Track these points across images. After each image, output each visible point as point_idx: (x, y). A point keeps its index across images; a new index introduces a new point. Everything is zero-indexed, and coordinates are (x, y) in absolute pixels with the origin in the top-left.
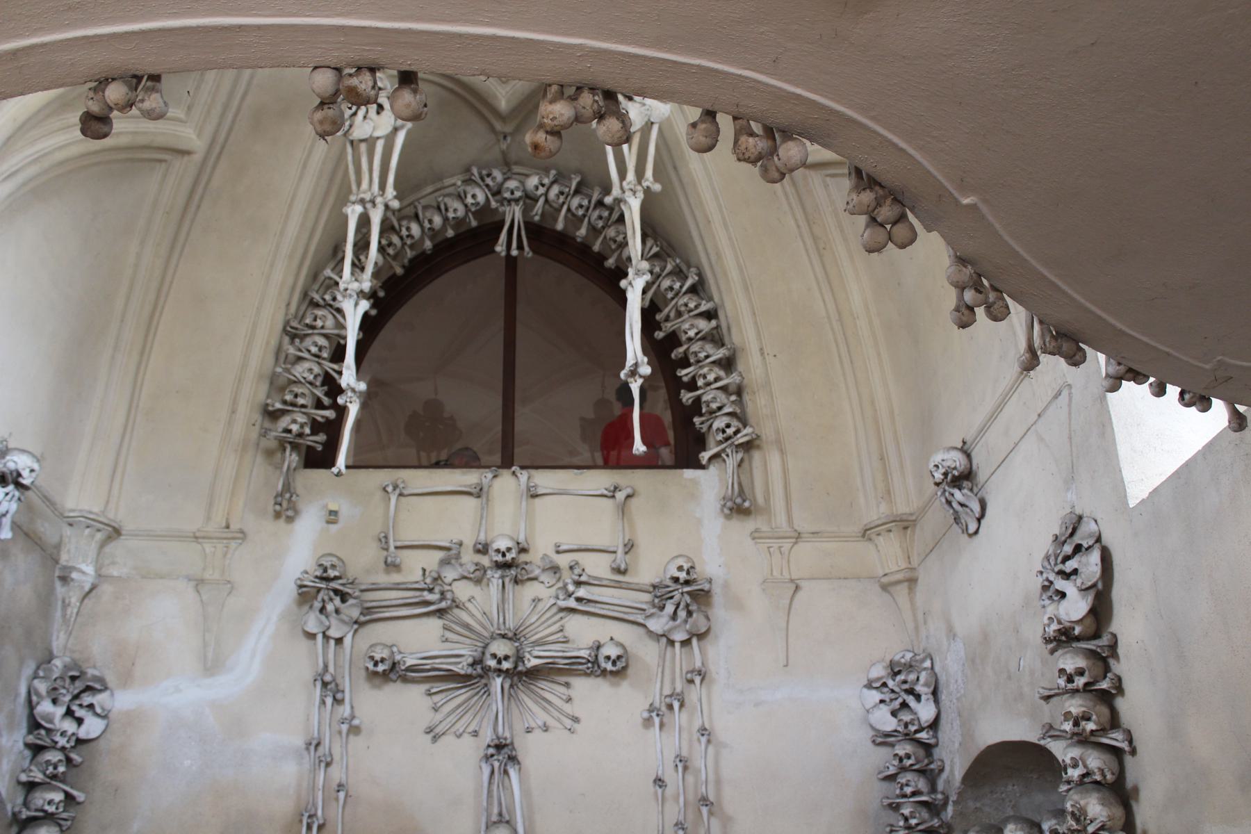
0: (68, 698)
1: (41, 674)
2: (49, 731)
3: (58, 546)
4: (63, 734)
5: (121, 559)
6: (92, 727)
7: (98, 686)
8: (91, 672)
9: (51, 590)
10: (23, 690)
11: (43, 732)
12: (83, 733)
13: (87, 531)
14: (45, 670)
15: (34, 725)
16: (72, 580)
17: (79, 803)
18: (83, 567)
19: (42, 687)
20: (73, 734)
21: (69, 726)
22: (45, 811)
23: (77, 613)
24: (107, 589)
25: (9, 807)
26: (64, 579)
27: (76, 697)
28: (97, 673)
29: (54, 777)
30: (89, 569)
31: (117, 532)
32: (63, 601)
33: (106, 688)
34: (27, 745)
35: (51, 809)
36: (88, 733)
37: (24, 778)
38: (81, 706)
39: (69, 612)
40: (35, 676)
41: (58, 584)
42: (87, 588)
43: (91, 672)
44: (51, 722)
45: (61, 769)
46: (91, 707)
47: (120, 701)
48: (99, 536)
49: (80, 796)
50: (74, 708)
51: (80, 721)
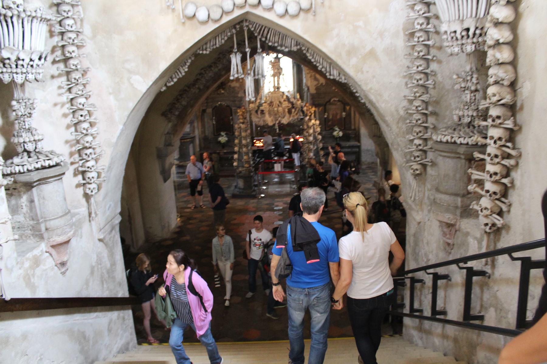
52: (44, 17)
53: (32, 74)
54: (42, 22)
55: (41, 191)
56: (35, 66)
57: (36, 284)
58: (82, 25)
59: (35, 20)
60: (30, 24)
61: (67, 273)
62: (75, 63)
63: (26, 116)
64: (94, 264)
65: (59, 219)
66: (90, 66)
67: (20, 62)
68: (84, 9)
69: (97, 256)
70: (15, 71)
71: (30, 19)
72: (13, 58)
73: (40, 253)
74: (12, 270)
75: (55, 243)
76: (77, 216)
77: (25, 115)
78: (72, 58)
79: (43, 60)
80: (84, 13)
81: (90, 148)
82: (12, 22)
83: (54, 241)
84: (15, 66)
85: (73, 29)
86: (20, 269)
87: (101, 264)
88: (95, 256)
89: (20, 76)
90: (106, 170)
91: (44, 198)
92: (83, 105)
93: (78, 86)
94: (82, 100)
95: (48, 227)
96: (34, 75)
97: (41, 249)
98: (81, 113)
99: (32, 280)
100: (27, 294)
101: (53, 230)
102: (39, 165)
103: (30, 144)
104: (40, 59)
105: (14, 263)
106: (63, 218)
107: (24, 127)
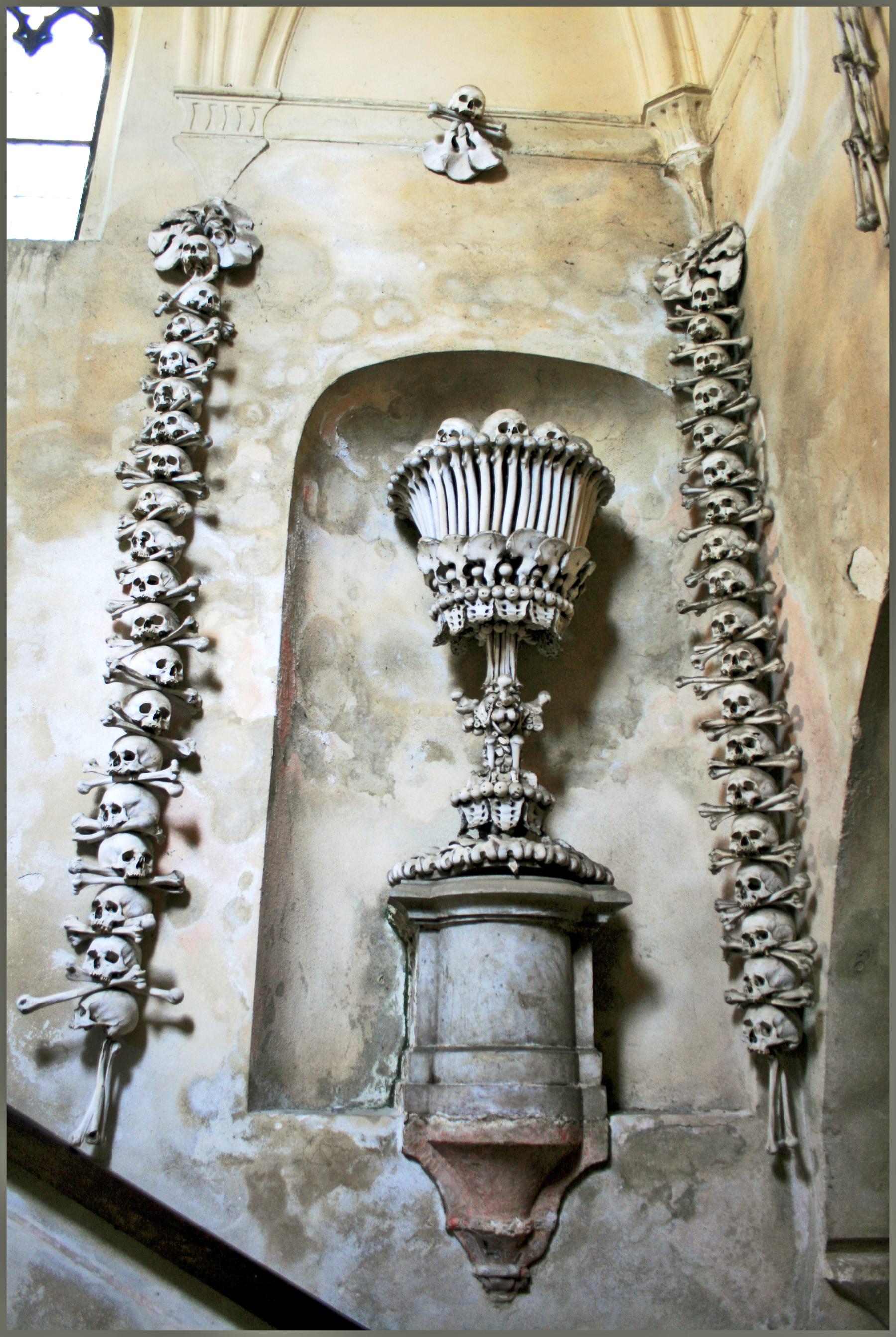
1: (664, 260)
2: (686, 302)
3: (655, 148)
4: (698, 294)
9: (662, 189)
11: (679, 307)
14: (673, 257)
15: (670, 306)
16: (673, 165)
18: (682, 147)
19: (668, 271)
21: (704, 285)
26: (670, 173)
27: (706, 252)
34: (673, 327)
36: (729, 279)
38: (709, 261)
39: (695, 195)
42: (697, 162)
46: (723, 255)
48: (681, 109)
57: (309, 1233)
59: (482, 459)
61: (522, 1301)
65: (466, 1055)
67: (450, 575)
73: (375, 1145)
74: (205, 1121)
79: (526, 566)
85: (722, 475)
86: (247, 1139)
95: (437, 1074)
96: (491, 607)
97: (384, 1132)
99: (293, 1207)
105: (225, 1107)
106: (485, 1056)
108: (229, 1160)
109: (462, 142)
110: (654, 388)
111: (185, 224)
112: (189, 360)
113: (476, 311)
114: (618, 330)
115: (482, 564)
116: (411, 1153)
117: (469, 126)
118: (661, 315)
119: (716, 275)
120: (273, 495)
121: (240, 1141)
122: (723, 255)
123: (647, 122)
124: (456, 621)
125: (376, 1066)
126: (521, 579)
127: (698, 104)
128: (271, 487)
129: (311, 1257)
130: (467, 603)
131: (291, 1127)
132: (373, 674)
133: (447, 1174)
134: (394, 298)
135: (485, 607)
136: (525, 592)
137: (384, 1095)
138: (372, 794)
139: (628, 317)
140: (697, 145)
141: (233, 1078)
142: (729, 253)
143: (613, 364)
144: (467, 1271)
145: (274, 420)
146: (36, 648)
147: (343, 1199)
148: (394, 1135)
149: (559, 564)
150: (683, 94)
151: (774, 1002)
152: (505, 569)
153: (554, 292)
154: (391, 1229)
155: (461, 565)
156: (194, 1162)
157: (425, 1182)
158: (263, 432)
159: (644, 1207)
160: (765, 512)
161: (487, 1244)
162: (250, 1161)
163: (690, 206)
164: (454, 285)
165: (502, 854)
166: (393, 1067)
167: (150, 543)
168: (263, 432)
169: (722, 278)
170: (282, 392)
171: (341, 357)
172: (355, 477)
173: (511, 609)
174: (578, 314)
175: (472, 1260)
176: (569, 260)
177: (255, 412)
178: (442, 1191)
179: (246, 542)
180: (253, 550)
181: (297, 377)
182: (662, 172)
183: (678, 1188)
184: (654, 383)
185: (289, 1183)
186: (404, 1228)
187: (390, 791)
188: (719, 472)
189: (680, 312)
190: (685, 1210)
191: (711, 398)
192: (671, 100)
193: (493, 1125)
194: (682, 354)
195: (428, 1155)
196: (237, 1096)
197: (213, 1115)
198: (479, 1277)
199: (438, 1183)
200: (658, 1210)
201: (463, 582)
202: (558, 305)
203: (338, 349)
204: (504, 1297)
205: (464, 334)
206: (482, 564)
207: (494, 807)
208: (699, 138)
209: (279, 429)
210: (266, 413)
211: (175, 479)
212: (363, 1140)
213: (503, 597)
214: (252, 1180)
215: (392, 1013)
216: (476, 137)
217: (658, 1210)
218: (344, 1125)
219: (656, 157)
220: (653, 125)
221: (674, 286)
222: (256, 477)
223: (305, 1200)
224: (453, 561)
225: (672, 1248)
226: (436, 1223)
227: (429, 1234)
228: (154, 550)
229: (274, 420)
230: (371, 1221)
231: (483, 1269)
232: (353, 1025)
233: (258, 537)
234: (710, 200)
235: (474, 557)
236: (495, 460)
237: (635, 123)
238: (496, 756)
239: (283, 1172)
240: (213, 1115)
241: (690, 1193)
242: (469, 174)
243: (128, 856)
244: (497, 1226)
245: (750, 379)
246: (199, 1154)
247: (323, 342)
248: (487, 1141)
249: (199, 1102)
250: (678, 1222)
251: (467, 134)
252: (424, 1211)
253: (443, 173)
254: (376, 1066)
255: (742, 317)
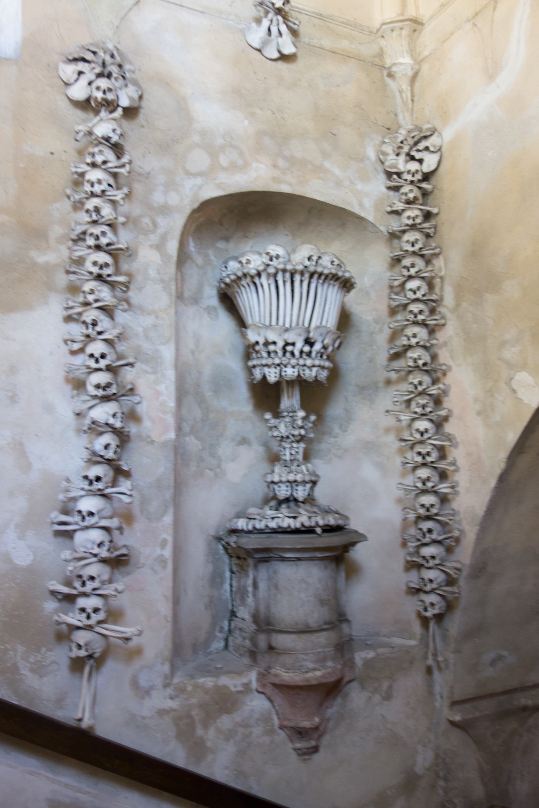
0: (406, 149)
1: (386, 140)
2: (399, 174)
3: (381, 54)
4: (409, 172)
5: (428, 39)
6: (430, 162)
7: (428, 134)
8: (426, 126)
9: (385, 86)
10: (371, 154)
11: (395, 176)
12: (427, 167)
13: (394, 34)
14: (390, 138)
15: (389, 175)
16: (395, 72)
17: (437, 214)
18: (401, 60)
19: (389, 149)
20: (417, 171)
21: (413, 166)
22: (407, 225)
23: (413, 95)
24: (425, 67)
25: (382, 228)
26: (390, 75)
27: (416, 144)
28: (429, 126)
29: (408, 202)
30: (407, 60)
31: (416, 24)
32: (400, 92)
33: (434, 132)
34: (389, 188)
35: (410, 222)
36: (429, 166)
37: (389, 209)
38: (418, 151)
39: (404, 95)
40: (384, 143)
41: (389, 81)
42: (410, 73)
43: (426, 126)
44: (395, 167)
45: (411, 196)
46: (427, 149)
47: (446, 136)
48: (404, 33)
49: (435, 210)
50: (413, 153)
51: (421, 161)
52: (312, 269)
53: (293, 367)
54: (327, 281)
55: (275, 573)
56: (297, 353)
57: (209, 744)
58: (442, 289)
59: (297, 278)
60: (288, 285)
61: (316, 757)
62: (415, 355)
63: (289, 440)
64: (419, 769)
65: (293, 636)
66: (450, 362)
67: (272, 348)
68: (446, 261)
69: (437, 756)
70: (264, 362)
71: (288, 275)
72: (261, 341)
73: (240, 688)
74: (147, 692)
75: (277, 681)
76: (381, 650)
77: (288, 437)
78: (410, 347)
79: (318, 347)
80: (446, 266)
81: (428, 518)
82: (262, 285)
83: (276, 675)
84: (265, 355)
85: (419, 295)
86: (172, 698)
87: (446, 780)
88: (430, 755)
89: (273, 370)
90: (465, 572)
91: (276, 587)
92: (422, 434)
93: (418, 398)
94: (422, 425)
95: (274, 644)
96: (296, 370)
97: (245, 681)
98: (418, 448)
99: (200, 732)
100: (177, 756)
101: (279, 654)
102: (273, 524)
103: (283, 487)
104: (309, 342)
105: (159, 682)
106: (304, 636)
107: (284, 458)
108: (162, 712)
109: (274, 30)
110: (377, 228)
111: (93, 65)
112: (110, 185)
113: (281, 163)
114: (360, 186)
115: (293, 344)
116: (261, 690)
117: (280, 18)
118: (382, 177)
119: (421, 161)
120: (164, 288)
121: (168, 700)
122: (427, 149)
123: (379, 34)
124: (273, 375)
125: (218, 629)
126: (313, 354)
127: (415, 31)
128: (162, 281)
129: (210, 757)
130: (282, 366)
131: (196, 686)
132: (208, 394)
133: (279, 700)
134: (232, 146)
135: (293, 370)
136: (317, 362)
137: (222, 644)
138: (210, 470)
139: (365, 178)
140: (411, 62)
141: (163, 664)
142: (432, 149)
143: (356, 209)
144: (288, 747)
145: (160, 231)
146: (10, 394)
147: (225, 721)
148: (250, 682)
149: (333, 346)
150: (408, 23)
151: (438, 592)
152: (307, 349)
153: (325, 155)
154: (251, 733)
155: (281, 344)
156: (144, 718)
157: (267, 704)
158: (154, 238)
159: (370, 698)
160: (443, 322)
161: (300, 733)
162: (174, 710)
163: (399, 101)
164: (267, 141)
165: (313, 524)
166: (226, 628)
167: (98, 329)
168: (154, 238)
169: (425, 164)
170: (165, 210)
171: (200, 187)
172: (197, 265)
173: (307, 372)
174: (337, 172)
175: (292, 741)
176: (333, 131)
177: (147, 224)
178: (277, 708)
179: (149, 321)
180: (155, 326)
181: (173, 199)
182: (385, 73)
183: (385, 685)
184: (377, 225)
185: (197, 718)
186: (257, 730)
187: (219, 466)
188: (418, 292)
189: (394, 179)
190: (388, 697)
191: (415, 245)
192: (400, 24)
193: (310, 675)
194: (395, 209)
195: (269, 690)
196: (166, 675)
197: (152, 688)
198: (295, 750)
199: (275, 704)
200: (377, 698)
201: (280, 353)
202: (327, 164)
203: (199, 181)
204: (307, 757)
205: (276, 180)
206: (293, 344)
207: (295, 487)
208: (412, 57)
209: (164, 238)
210: (155, 225)
211: (109, 279)
212: (235, 687)
213: (304, 365)
214: (176, 721)
215: (224, 597)
216: (283, 28)
217: (377, 698)
218: (225, 681)
219: (381, 61)
220: (383, 37)
221: (394, 161)
222: (152, 273)
223: (206, 726)
224: (276, 340)
225: (383, 716)
226: (273, 725)
227: (271, 732)
228: (100, 333)
229: (160, 231)
230: (240, 730)
231: (298, 745)
232: (206, 608)
233: (157, 317)
234: (413, 100)
235: (290, 341)
236: (305, 280)
237: (371, 32)
238: (291, 454)
239: (193, 713)
240: (152, 688)
241: (390, 687)
242: (276, 55)
243: (100, 545)
244: (306, 724)
245: (435, 233)
246: (146, 712)
247: (189, 174)
248: (308, 684)
249: (143, 682)
250: (386, 703)
251: (278, 25)
252: (266, 719)
253: (259, 50)
254: (218, 629)
255: (431, 192)
